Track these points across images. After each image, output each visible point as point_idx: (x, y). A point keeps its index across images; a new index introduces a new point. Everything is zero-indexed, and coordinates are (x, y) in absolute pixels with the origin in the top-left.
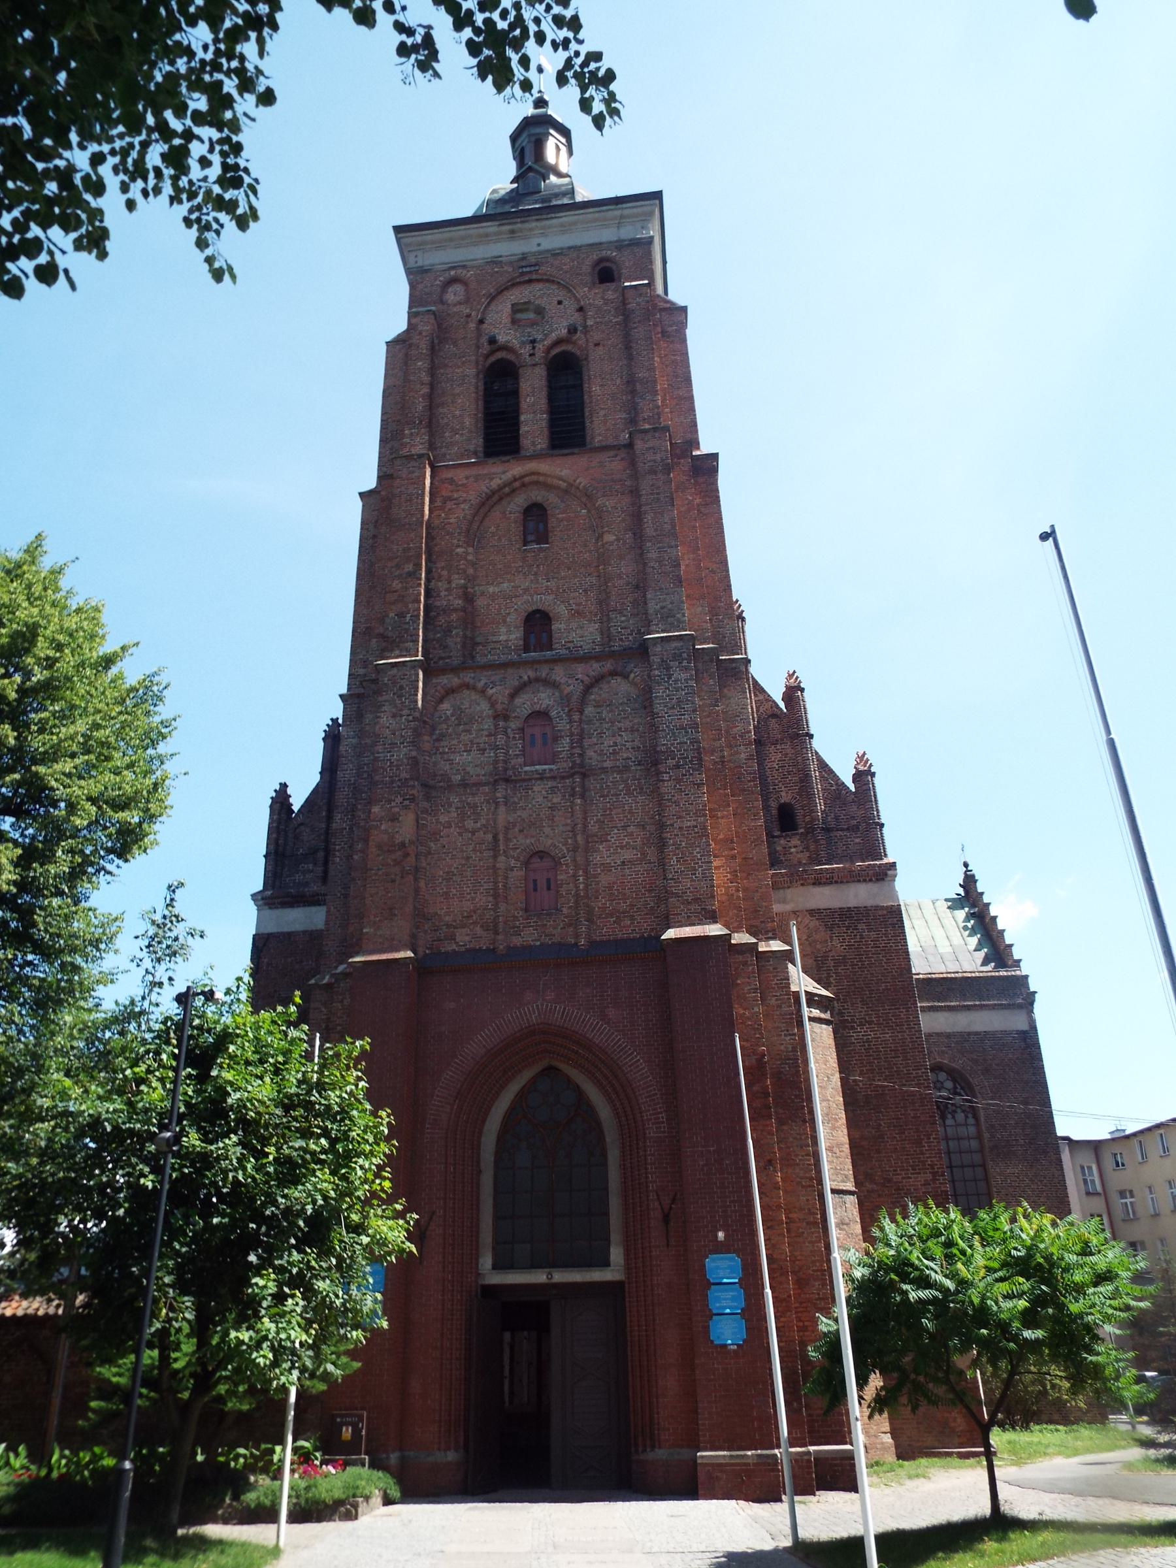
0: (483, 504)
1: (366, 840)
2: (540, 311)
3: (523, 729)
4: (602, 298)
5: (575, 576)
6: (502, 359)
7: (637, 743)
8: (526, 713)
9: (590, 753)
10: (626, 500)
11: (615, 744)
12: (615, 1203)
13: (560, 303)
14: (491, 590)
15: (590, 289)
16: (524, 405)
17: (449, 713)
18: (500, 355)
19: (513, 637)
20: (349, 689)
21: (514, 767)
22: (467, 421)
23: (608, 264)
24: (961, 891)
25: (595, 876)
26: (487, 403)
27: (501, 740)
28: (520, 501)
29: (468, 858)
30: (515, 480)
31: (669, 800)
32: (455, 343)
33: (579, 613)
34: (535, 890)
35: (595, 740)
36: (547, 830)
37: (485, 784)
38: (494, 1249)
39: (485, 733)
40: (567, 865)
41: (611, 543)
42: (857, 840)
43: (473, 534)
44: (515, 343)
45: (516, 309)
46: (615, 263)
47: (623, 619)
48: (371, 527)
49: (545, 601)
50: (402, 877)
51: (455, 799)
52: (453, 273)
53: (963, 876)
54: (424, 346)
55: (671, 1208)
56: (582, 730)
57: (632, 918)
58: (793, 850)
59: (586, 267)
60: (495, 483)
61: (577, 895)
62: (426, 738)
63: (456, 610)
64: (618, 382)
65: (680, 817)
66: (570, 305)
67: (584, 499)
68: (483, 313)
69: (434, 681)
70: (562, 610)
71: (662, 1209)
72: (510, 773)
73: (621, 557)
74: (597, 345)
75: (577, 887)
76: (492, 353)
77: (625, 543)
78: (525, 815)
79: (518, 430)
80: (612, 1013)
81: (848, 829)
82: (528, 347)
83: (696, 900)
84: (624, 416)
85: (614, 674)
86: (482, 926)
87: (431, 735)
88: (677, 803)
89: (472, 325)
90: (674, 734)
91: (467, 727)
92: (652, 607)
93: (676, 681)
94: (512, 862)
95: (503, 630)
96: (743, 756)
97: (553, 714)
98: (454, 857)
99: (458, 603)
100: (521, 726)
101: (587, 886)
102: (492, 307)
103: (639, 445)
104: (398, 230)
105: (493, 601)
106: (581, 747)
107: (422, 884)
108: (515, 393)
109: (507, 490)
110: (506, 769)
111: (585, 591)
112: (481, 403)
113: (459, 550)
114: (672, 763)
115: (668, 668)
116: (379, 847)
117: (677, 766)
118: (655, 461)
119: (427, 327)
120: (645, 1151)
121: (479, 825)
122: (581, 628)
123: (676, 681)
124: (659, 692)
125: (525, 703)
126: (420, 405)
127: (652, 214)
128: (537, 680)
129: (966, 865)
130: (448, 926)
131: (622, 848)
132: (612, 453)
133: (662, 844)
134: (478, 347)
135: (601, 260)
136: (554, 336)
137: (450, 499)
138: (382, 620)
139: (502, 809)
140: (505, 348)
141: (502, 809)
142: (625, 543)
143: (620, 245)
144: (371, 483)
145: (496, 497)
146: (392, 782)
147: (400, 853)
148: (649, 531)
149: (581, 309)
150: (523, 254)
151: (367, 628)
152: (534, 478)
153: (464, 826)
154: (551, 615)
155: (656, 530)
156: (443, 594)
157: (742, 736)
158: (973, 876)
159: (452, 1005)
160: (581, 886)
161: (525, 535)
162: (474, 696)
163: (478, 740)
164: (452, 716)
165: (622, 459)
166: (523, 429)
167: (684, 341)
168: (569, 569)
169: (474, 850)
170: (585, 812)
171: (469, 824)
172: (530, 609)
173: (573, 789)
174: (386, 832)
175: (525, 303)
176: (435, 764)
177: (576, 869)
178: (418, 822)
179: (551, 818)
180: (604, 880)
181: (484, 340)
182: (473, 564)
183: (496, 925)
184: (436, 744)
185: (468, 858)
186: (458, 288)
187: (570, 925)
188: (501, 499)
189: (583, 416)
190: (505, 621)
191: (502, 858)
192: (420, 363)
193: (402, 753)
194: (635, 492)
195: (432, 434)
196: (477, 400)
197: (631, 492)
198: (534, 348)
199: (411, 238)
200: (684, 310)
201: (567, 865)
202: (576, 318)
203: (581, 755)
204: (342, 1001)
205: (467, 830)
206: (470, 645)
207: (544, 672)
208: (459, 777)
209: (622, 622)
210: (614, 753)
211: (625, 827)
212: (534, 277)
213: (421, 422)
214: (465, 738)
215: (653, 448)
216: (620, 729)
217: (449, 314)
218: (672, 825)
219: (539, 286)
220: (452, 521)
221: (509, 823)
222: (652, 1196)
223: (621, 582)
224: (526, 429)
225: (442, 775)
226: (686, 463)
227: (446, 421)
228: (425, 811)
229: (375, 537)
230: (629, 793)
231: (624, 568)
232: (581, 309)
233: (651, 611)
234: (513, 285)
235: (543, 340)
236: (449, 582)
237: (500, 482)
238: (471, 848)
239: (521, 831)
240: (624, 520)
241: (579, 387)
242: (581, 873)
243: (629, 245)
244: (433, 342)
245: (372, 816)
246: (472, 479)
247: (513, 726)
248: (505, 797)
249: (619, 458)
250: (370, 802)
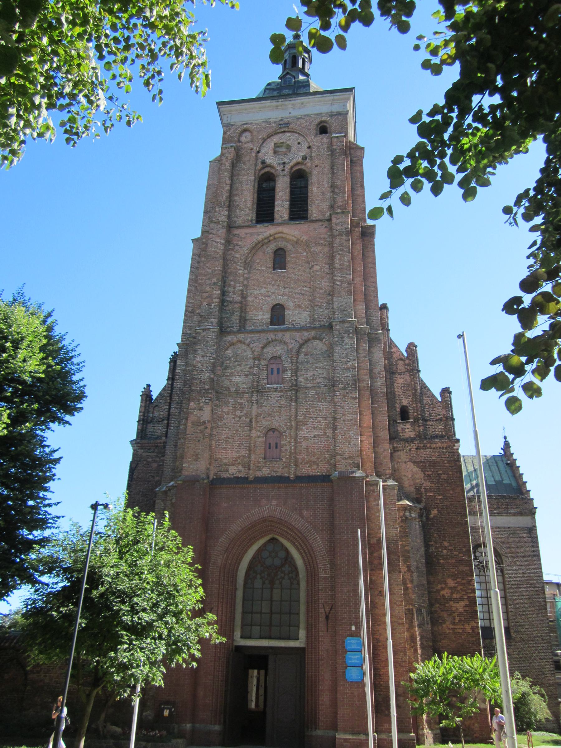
0: (253, 248)
1: (187, 419)
2: (289, 147)
3: (267, 365)
4: (321, 142)
5: (298, 287)
6: (268, 172)
7: (325, 375)
8: (270, 357)
9: (301, 379)
10: (326, 249)
11: (314, 375)
12: (303, 608)
13: (299, 143)
14: (256, 292)
15: (315, 137)
16: (277, 197)
17: (231, 355)
18: (266, 170)
19: (265, 317)
20: (182, 341)
21: (262, 385)
22: (249, 204)
23: (325, 124)
24: (502, 452)
25: (300, 443)
26: (258, 194)
27: (256, 370)
28: (273, 247)
29: (237, 431)
30: (271, 236)
31: (339, 406)
32: (244, 163)
33: (299, 306)
34: (270, 448)
35: (303, 372)
36: (277, 418)
37: (247, 393)
38: (241, 628)
39: (248, 366)
40: (286, 436)
41: (318, 271)
42: (440, 427)
43: (248, 265)
44: (275, 164)
45: (276, 146)
46: (327, 123)
47: (321, 310)
48: (197, 257)
49: (282, 300)
50: (203, 439)
51: (232, 400)
52: (245, 126)
53: (503, 444)
54: (228, 165)
55: (329, 613)
56: (297, 368)
57: (318, 465)
58: (407, 430)
59: (313, 126)
60: (260, 238)
61: (290, 452)
62: (219, 368)
63: (237, 302)
64: (326, 186)
65: (344, 415)
66: (304, 145)
67: (305, 247)
68: (260, 148)
69: (224, 339)
70: (290, 304)
71: (326, 613)
72: (260, 387)
73: (322, 278)
74: (316, 166)
75: (291, 448)
76: (263, 168)
77: (324, 271)
78: (266, 409)
79: (273, 210)
80: (305, 513)
81: (436, 421)
82: (282, 166)
83: (350, 458)
84: (328, 204)
85: (314, 338)
86: (242, 465)
87: (221, 366)
88: (343, 407)
89: (254, 154)
90: (343, 372)
91: (240, 363)
92: (336, 306)
93: (346, 344)
94: (259, 434)
95: (260, 313)
96: (379, 384)
97: (283, 358)
98: (230, 430)
99: (239, 299)
100: (266, 364)
101: (296, 447)
102: (264, 144)
103: (334, 221)
104: (219, 104)
105: (256, 298)
106: (296, 376)
107: (213, 442)
108: (273, 190)
109: (266, 241)
110: (258, 386)
111: (303, 295)
112: (256, 195)
113: (241, 272)
114: (341, 386)
115: (342, 338)
116: (193, 423)
117: (344, 389)
118: (342, 229)
119: (231, 155)
120: (318, 583)
121: (243, 414)
122: (300, 314)
123: (346, 344)
124: (337, 349)
125: (270, 351)
126: (225, 195)
127: (349, 99)
128: (276, 340)
129: (505, 438)
130: (226, 464)
131: (314, 428)
132: (320, 224)
133: (334, 428)
134: (256, 165)
135: (321, 122)
136: (294, 161)
137: (237, 245)
138: (199, 307)
139: (255, 406)
140: (270, 166)
141: (255, 406)
142: (324, 271)
143: (332, 115)
144: (198, 235)
145: (260, 245)
146: (201, 390)
147: (203, 427)
148: (337, 266)
149: (309, 147)
151: (192, 310)
152: (280, 235)
153: (235, 414)
154: (285, 307)
155: (340, 265)
156: (231, 294)
157: (379, 373)
158: (508, 444)
159: (225, 505)
160: (293, 448)
161: (274, 265)
162: (244, 347)
163: (244, 370)
164: (232, 357)
165: (326, 227)
166: (276, 209)
167: (362, 165)
168: (296, 283)
169: (240, 427)
170: (296, 409)
171: (238, 413)
172: (275, 304)
173: (291, 397)
174: (196, 415)
175: (281, 143)
176: (223, 381)
177: (291, 438)
178: (212, 411)
179: (279, 412)
180: (305, 445)
181: (259, 161)
182: (247, 279)
183: (249, 465)
184: (224, 371)
185: (237, 431)
186: (248, 134)
187: (286, 467)
188: (263, 245)
189: (307, 204)
190: (261, 309)
191: (253, 431)
192: (226, 174)
193: (206, 376)
194: (331, 245)
195: (230, 211)
196: (254, 193)
197: (329, 244)
198: (284, 167)
199: (224, 108)
200: (363, 149)
201: (286, 436)
202: (307, 152)
203: (296, 380)
204: (171, 500)
205: (237, 416)
206: (243, 320)
207: (280, 335)
208: (234, 389)
209: (321, 312)
210: (313, 379)
211: (316, 418)
212: (287, 130)
213: (224, 204)
214: (238, 369)
215: (341, 222)
216: (316, 367)
217: (242, 148)
218: (340, 418)
219: (289, 134)
220: (237, 256)
221: (258, 413)
222: (321, 606)
223: (321, 291)
224: (278, 209)
225: (225, 387)
226: (358, 230)
227: (237, 203)
228: (217, 406)
229: (198, 262)
230: (319, 400)
231: (325, 284)
232: (309, 147)
233: (335, 307)
234: (276, 133)
235: (289, 163)
236: (235, 288)
237: (263, 237)
238: (238, 425)
239: (264, 418)
240: (325, 259)
241: (306, 187)
242: (293, 440)
243: (336, 115)
244: (233, 163)
245: (190, 407)
246: (249, 235)
247: (263, 364)
248: (257, 400)
249: (324, 226)
250: (189, 400)
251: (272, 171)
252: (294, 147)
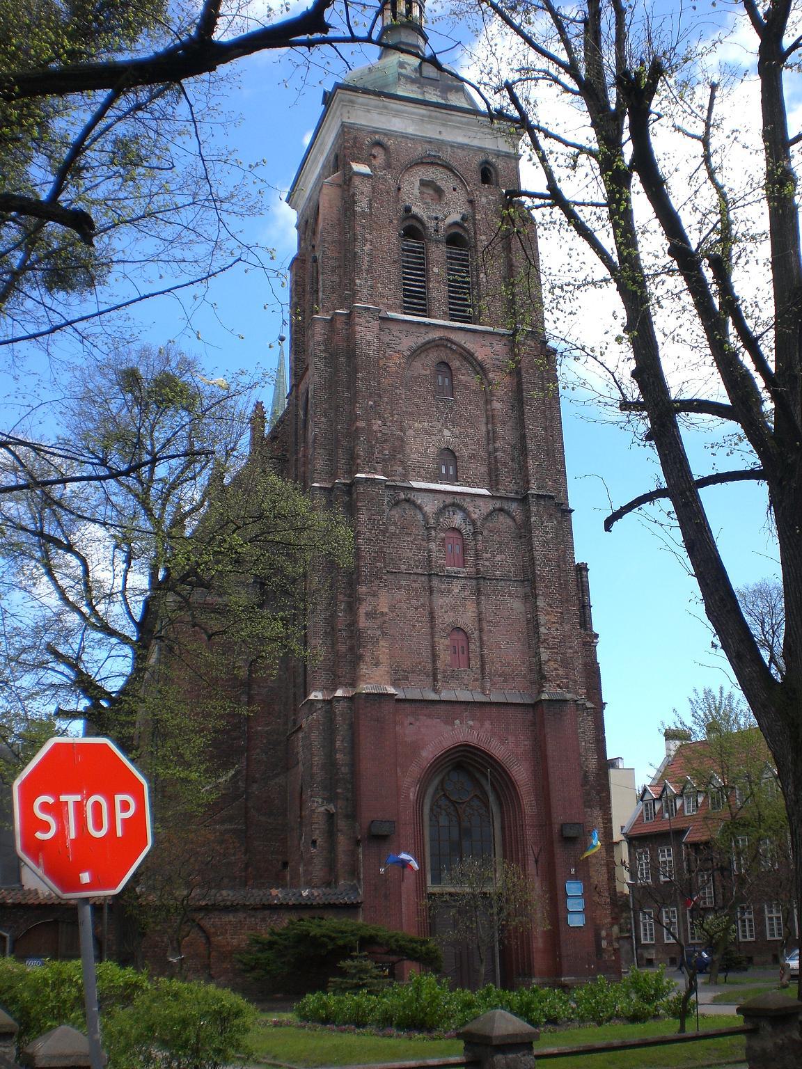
2: (439, 192)
46: (491, 166)
140: (415, 217)
143: (498, 154)
150: (430, 138)
171: (414, 602)
175: (429, 181)
243: (505, 156)
251: (418, 225)
252: (449, 195)
